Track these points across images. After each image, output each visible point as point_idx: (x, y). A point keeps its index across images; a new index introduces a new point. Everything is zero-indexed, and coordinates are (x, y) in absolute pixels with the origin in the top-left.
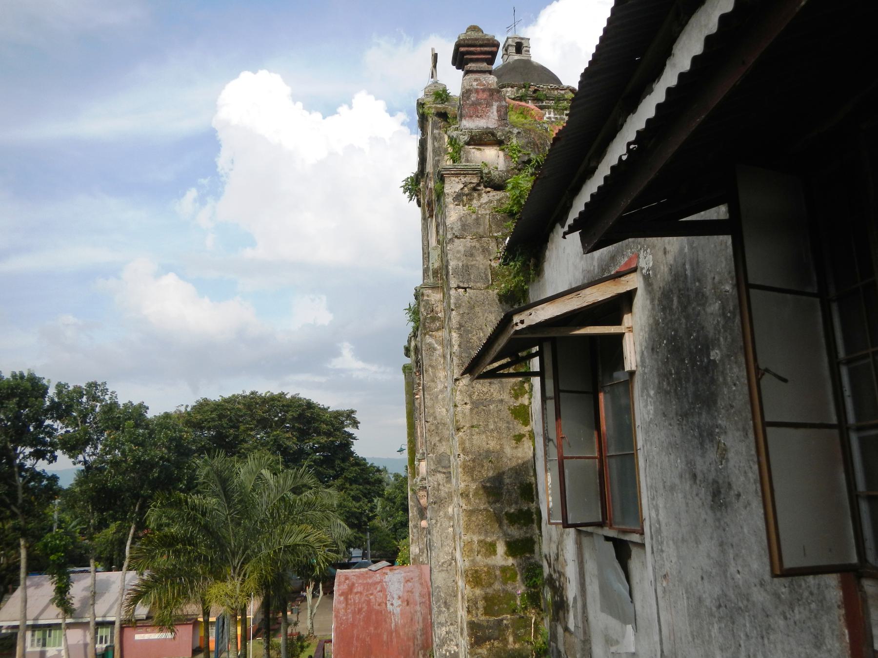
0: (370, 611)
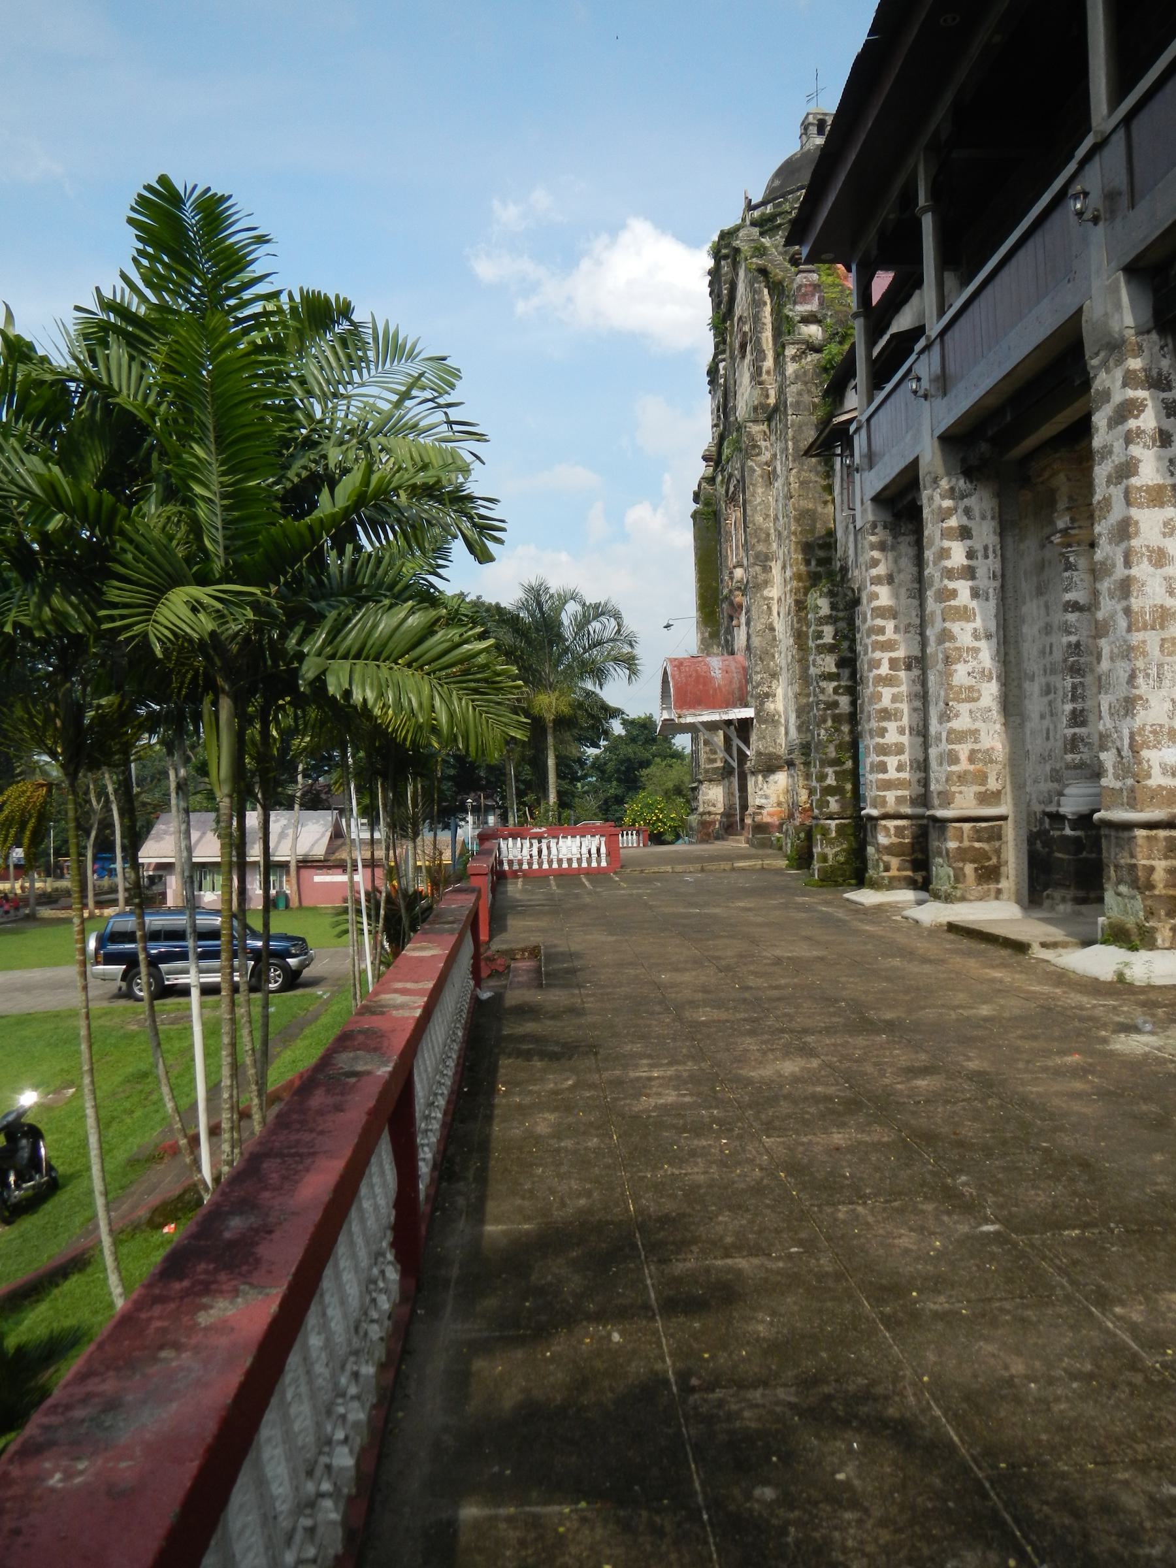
0: (698, 677)
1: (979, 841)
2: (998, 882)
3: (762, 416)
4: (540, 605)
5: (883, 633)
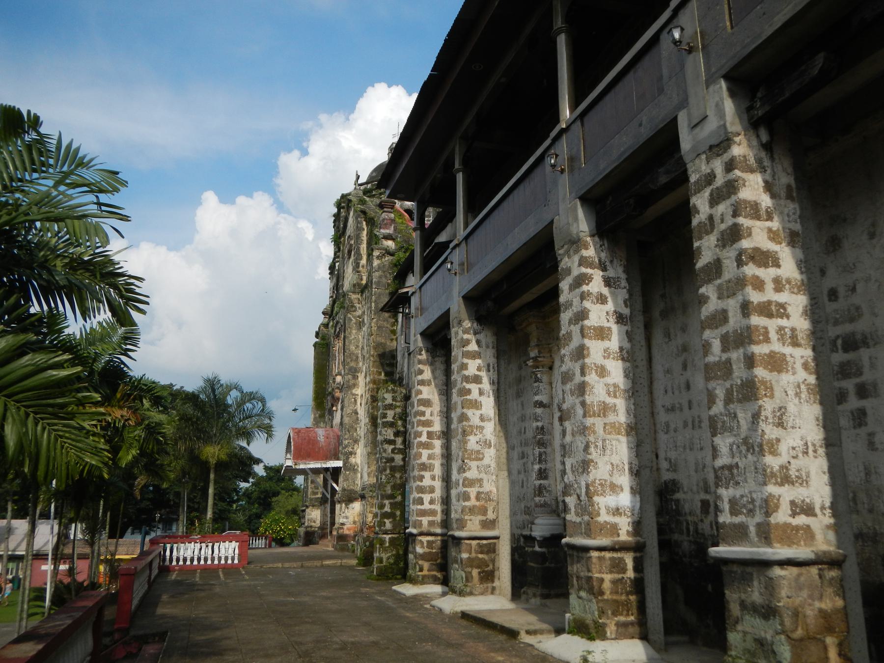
1: (481, 553)
2: (493, 582)
3: (357, 290)
4: (213, 390)
5: (424, 416)
